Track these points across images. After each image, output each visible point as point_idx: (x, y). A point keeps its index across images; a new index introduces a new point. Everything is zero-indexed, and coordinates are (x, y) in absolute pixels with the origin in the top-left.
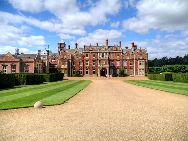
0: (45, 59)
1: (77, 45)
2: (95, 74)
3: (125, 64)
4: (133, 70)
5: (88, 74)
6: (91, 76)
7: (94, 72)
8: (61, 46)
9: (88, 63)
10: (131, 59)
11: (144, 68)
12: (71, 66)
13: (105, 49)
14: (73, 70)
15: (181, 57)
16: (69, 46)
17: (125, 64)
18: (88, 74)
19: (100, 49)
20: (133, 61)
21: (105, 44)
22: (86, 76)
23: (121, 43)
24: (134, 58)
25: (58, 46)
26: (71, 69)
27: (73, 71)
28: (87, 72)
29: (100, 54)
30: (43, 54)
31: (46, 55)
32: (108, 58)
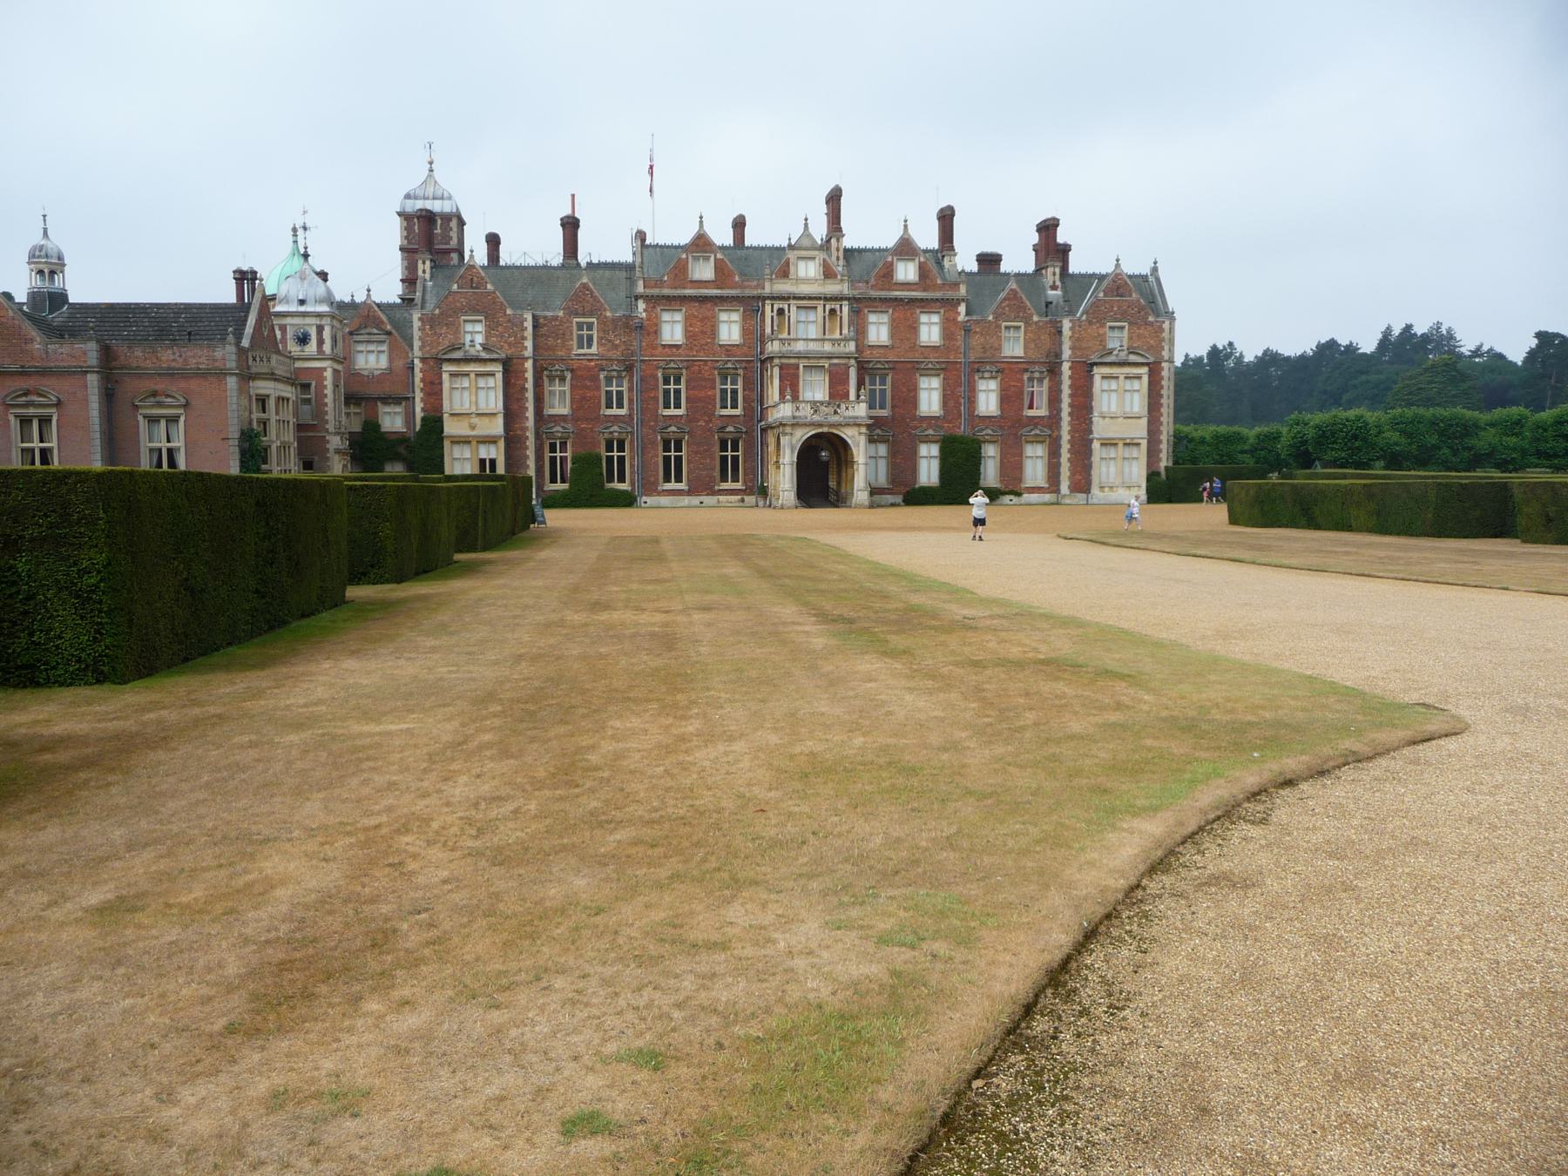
0: (312, 347)
1: (571, 226)
2: (739, 485)
3: (988, 400)
4: (1054, 453)
5: (682, 486)
6: (709, 500)
7: (727, 469)
8: (429, 234)
9: (678, 392)
10: (1034, 356)
11: (1145, 434)
12: (530, 414)
13: (828, 273)
14: (553, 449)
15: (1351, 349)
16: (493, 241)
17: (988, 400)
18: (682, 486)
20: (1053, 370)
21: (819, 231)
22: (665, 500)
23: (946, 218)
24: (1067, 353)
25: (393, 234)
26: (531, 443)
27: (553, 460)
28: (672, 470)
29: (781, 312)
30: (294, 308)
31: (319, 315)
32: (852, 347)
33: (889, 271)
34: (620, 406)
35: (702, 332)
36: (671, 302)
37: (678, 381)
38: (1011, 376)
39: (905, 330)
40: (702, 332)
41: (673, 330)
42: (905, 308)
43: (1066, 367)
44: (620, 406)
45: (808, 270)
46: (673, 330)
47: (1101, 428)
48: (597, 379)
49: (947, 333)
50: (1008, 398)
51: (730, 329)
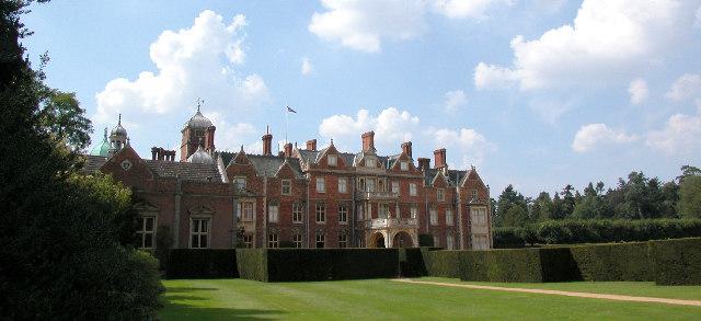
3: (434, 220)
12: (265, 223)
17: (434, 220)
19: (363, 164)
20: (454, 206)
33: (398, 166)
34: (300, 220)
35: (332, 187)
36: (319, 174)
37: (323, 209)
38: (441, 209)
39: (405, 190)
40: (332, 187)
41: (321, 186)
42: (405, 182)
43: (460, 205)
44: (300, 220)
45: (370, 163)
46: (321, 186)
47: (475, 230)
48: (290, 207)
49: (419, 192)
50: (442, 218)
51: (342, 187)
